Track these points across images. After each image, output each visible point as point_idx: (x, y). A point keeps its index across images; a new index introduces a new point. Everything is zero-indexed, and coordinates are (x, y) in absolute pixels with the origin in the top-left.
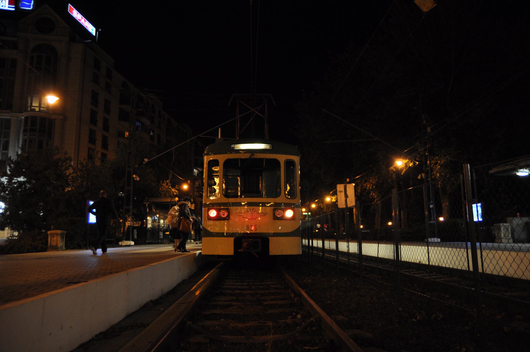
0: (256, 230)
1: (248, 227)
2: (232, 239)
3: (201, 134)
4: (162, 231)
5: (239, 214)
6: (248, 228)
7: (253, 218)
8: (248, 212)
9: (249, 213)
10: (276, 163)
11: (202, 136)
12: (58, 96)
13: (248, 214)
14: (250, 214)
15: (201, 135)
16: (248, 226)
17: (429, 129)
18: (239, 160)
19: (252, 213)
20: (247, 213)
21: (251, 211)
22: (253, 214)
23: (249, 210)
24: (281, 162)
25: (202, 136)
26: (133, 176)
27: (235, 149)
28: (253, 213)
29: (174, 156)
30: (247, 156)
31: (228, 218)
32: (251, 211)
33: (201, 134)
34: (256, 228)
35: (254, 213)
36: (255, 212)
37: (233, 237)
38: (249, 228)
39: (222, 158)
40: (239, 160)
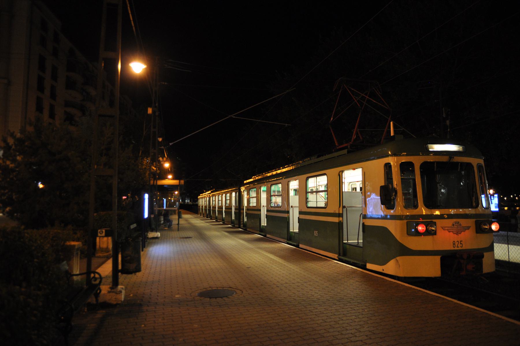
0: (462, 246)
1: (454, 243)
2: (438, 259)
3: (233, 115)
4: (162, 215)
5: (444, 228)
6: (455, 244)
7: (459, 232)
8: (454, 226)
9: (455, 226)
10: (469, 166)
11: (234, 117)
12: (145, 64)
13: (454, 228)
14: (456, 228)
15: (233, 116)
16: (454, 241)
17: (448, 122)
18: (435, 163)
19: (457, 227)
20: (453, 226)
21: (456, 224)
22: (458, 228)
23: (454, 224)
24: (474, 167)
25: (234, 117)
26: (159, 159)
27: (430, 150)
28: (458, 226)
29: (145, 131)
30: (445, 159)
31: (434, 233)
32: (456, 224)
33: (233, 115)
34: (462, 244)
35: (459, 226)
36: (460, 225)
37: (440, 255)
38: (455, 244)
39: (417, 161)
40: (435, 163)
